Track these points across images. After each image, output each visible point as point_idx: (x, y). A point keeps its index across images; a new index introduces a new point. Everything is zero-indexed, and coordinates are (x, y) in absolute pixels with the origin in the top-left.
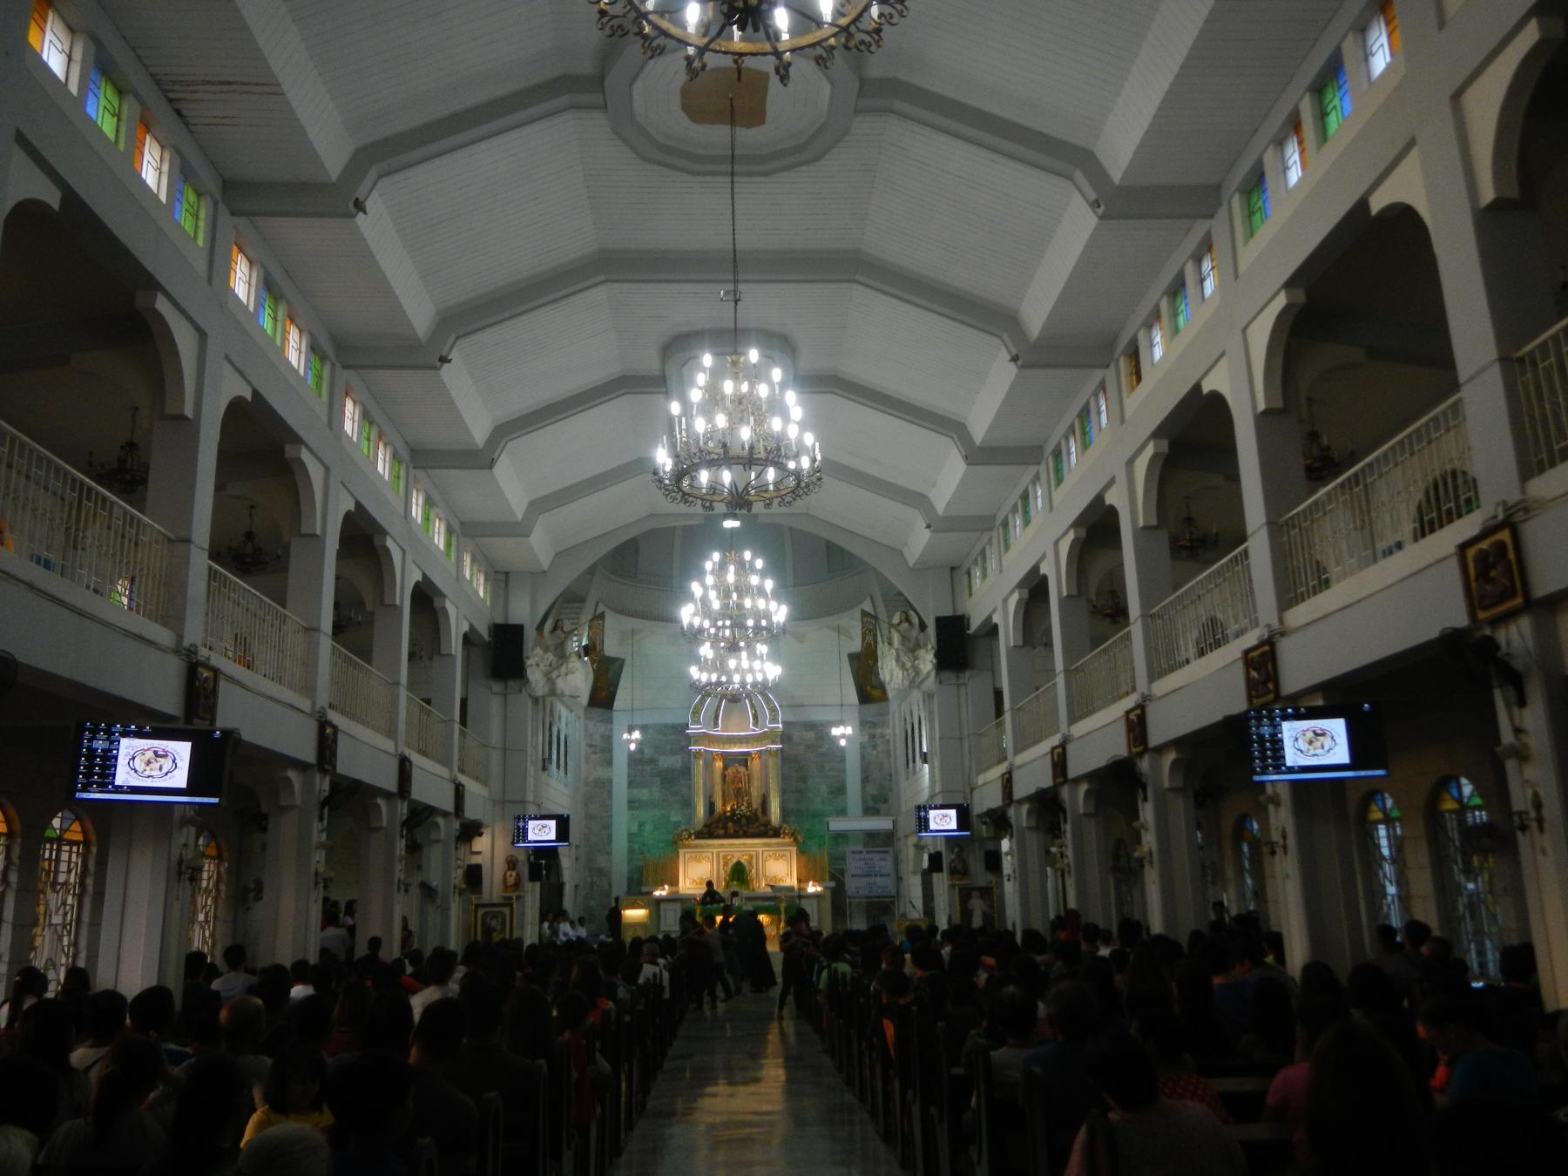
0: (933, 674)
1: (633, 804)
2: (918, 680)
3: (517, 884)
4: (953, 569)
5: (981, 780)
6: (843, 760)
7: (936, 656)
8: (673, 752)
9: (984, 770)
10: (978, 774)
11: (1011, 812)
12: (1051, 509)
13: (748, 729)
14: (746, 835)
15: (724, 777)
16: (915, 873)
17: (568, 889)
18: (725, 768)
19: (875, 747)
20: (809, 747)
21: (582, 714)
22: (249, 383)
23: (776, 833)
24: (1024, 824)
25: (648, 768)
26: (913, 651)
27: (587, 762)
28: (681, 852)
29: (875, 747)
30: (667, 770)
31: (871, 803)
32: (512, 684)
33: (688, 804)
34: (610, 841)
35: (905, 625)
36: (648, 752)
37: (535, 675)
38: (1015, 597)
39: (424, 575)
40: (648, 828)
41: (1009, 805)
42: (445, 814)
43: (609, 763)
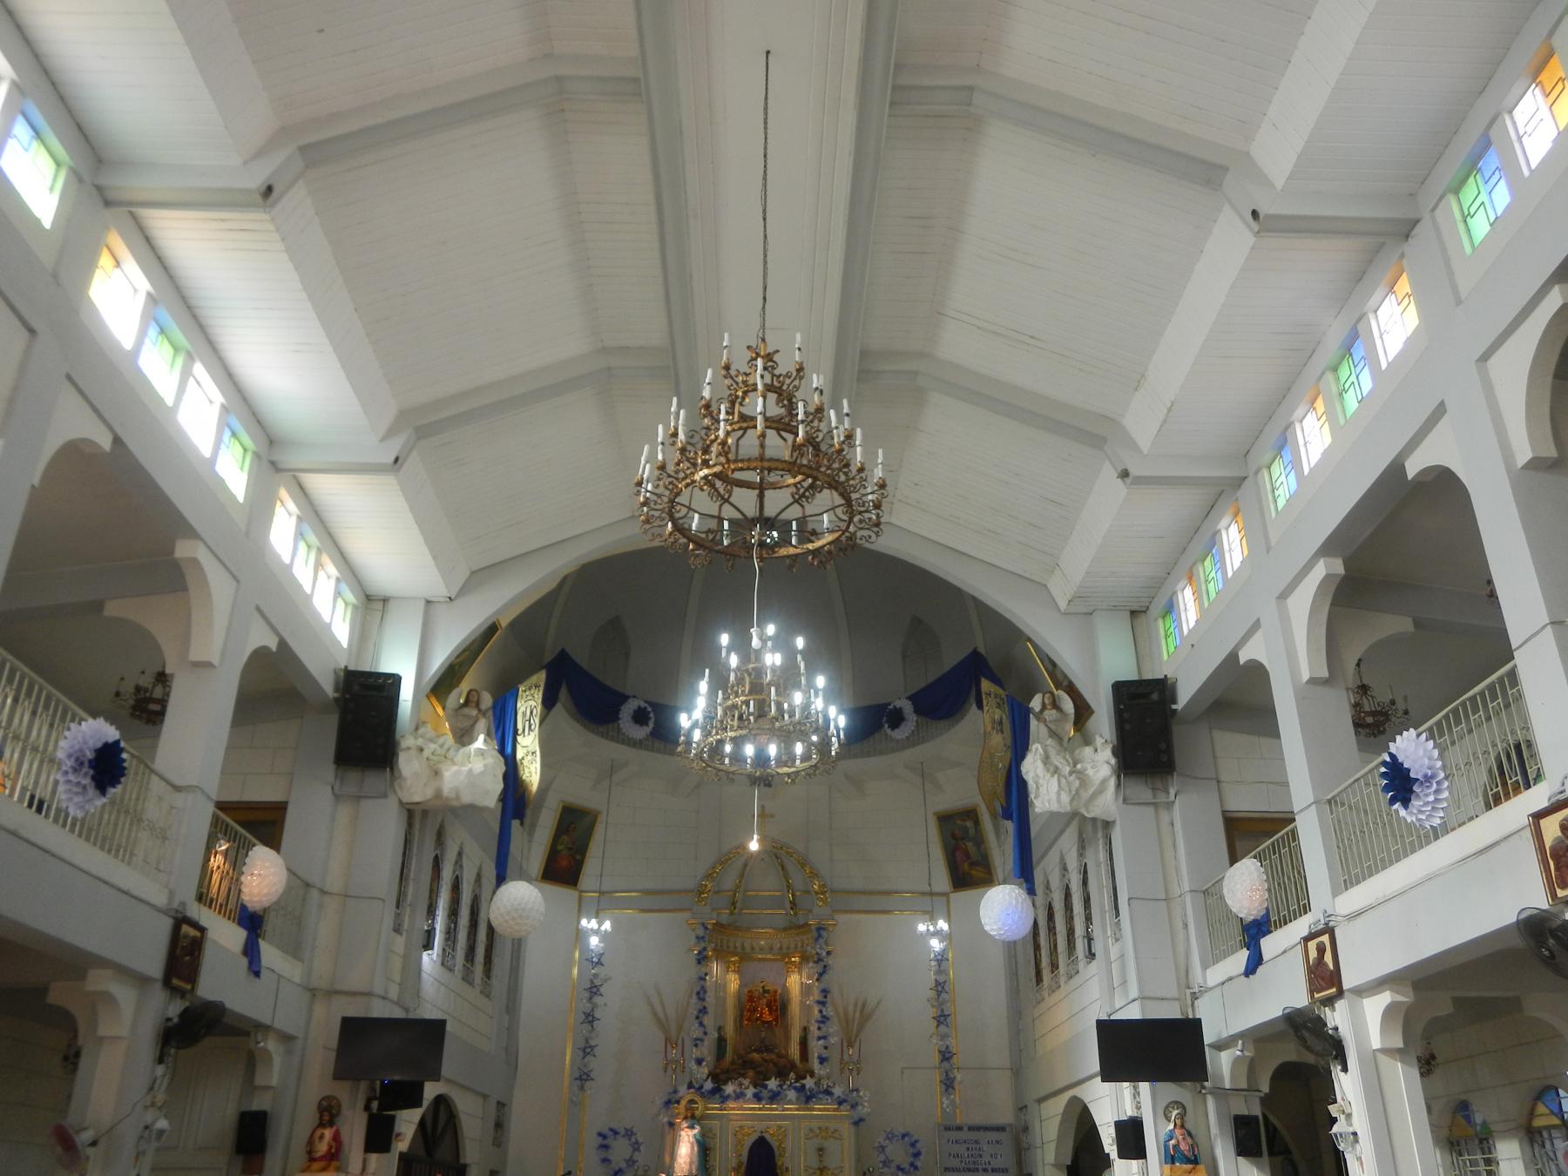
0: (1112, 782)
2: (1085, 795)
3: (334, 1156)
4: (1133, 613)
5: (1216, 974)
7: (1115, 753)
9: (1216, 961)
10: (1205, 967)
11: (1338, 1018)
12: (1459, 302)
22: (110, 428)
24: (1376, 1042)
26: (1072, 753)
32: (374, 780)
35: (1050, 714)
37: (408, 764)
38: (1320, 571)
39: (117, 441)
41: (1329, 1002)
42: (142, 980)
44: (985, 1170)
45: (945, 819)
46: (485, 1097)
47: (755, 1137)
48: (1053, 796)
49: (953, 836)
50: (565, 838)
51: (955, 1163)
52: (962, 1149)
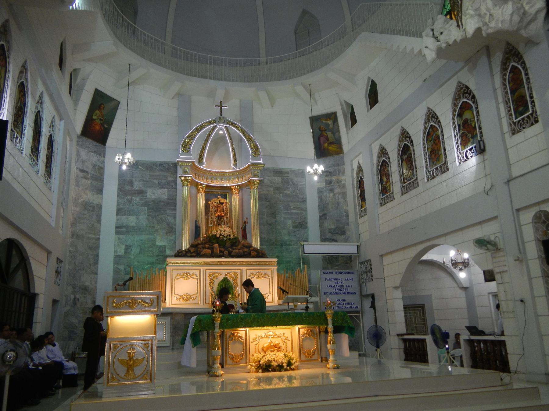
1: (120, 229)
6: (304, 201)
8: (161, 186)
13: (230, 168)
14: (230, 255)
15: (207, 206)
16: (396, 288)
17: (42, 305)
18: (207, 200)
19: (331, 190)
20: (277, 189)
21: (75, 140)
23: (259, 254)
25: (136, 199)
27: (77, 185)
28: (169, 269)
29: (331, 190)
30: (154, 201)
31: (329, 236)
33: (171, 230)
34: (96, 262)
36: (137, 185)
40: (135, 251)
43: (100, 191)
44: (344, 293)
45: (314, 120)
46: (49, 253)
47: (221, 278)
48: (507, 17)
49: (320, 129)
50: (97, 112)
51: (331, 290)
52: (332, 283)
